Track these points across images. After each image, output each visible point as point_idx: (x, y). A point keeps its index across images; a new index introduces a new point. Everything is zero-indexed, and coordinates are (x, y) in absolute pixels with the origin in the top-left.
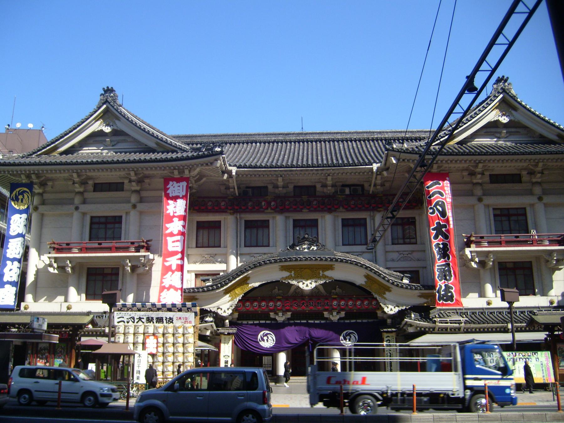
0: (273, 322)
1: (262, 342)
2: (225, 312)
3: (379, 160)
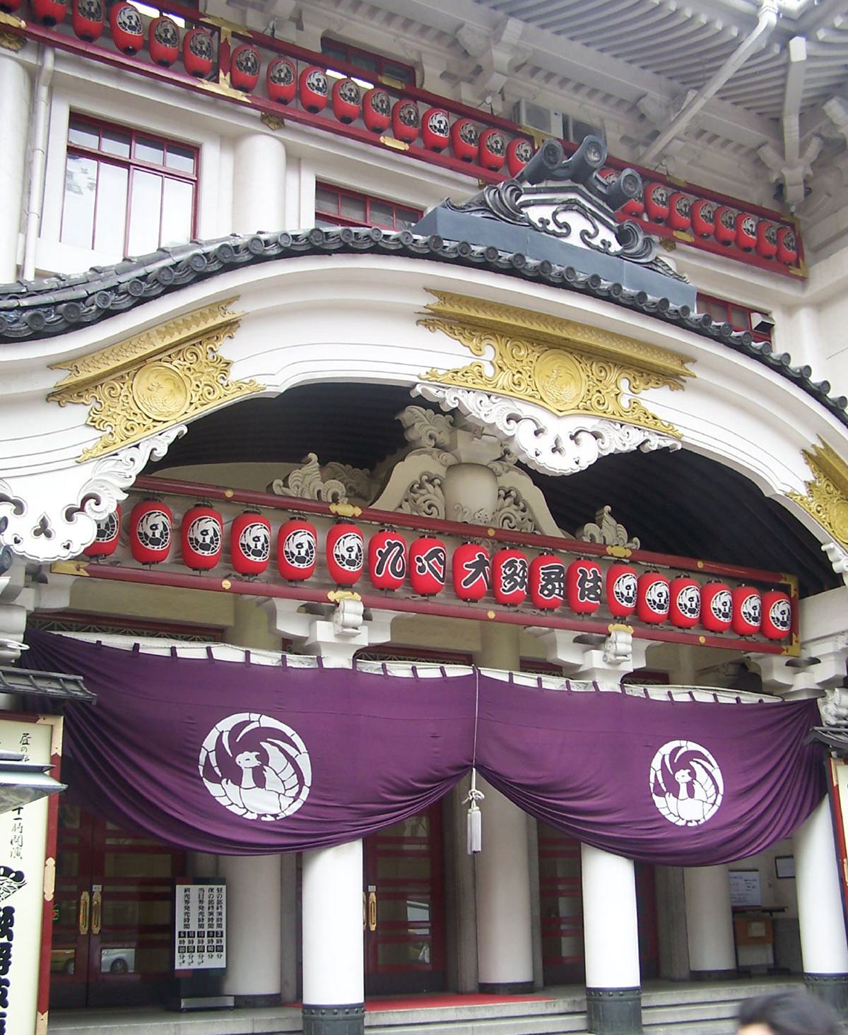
0: (295, 661)
1: (670, 798)
2: (43, 529)
3: (778, 67)
